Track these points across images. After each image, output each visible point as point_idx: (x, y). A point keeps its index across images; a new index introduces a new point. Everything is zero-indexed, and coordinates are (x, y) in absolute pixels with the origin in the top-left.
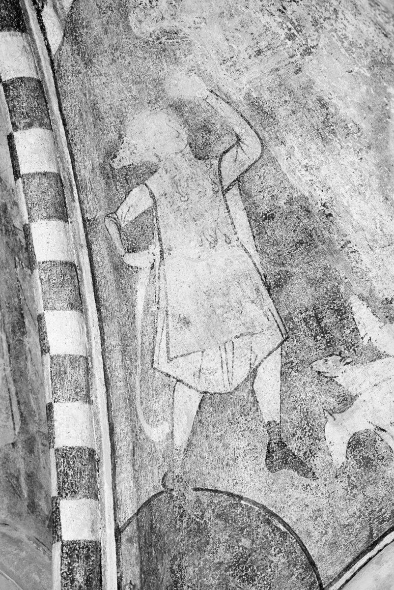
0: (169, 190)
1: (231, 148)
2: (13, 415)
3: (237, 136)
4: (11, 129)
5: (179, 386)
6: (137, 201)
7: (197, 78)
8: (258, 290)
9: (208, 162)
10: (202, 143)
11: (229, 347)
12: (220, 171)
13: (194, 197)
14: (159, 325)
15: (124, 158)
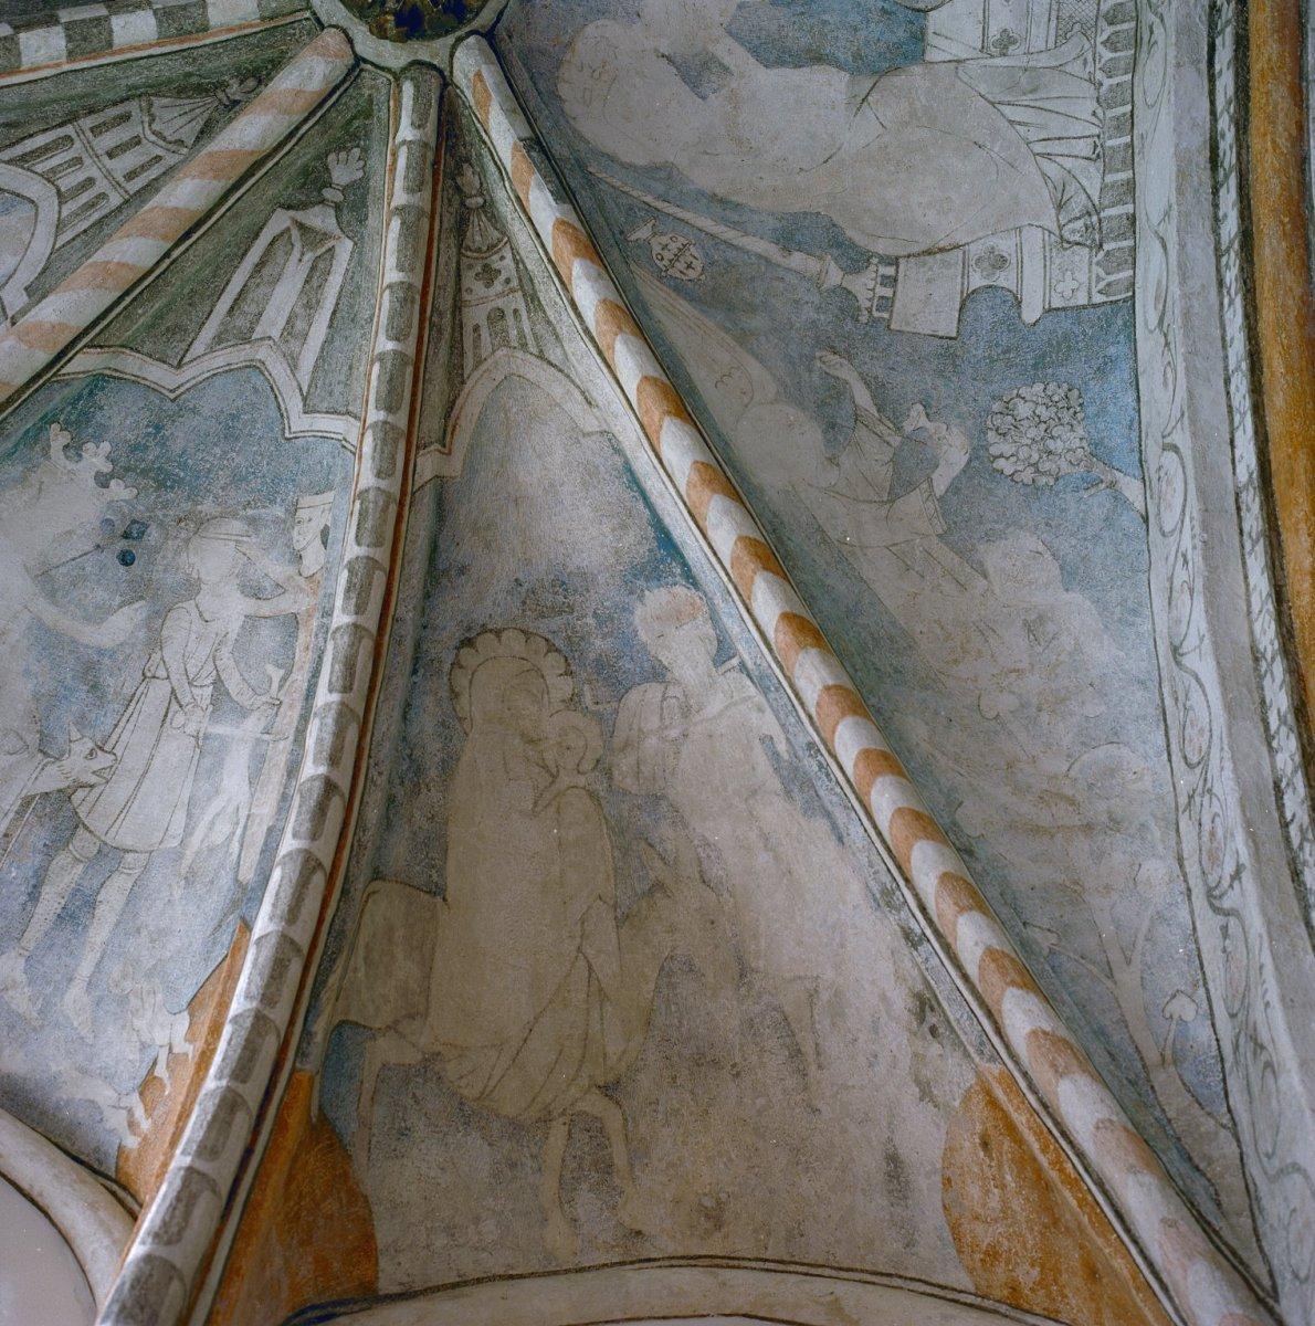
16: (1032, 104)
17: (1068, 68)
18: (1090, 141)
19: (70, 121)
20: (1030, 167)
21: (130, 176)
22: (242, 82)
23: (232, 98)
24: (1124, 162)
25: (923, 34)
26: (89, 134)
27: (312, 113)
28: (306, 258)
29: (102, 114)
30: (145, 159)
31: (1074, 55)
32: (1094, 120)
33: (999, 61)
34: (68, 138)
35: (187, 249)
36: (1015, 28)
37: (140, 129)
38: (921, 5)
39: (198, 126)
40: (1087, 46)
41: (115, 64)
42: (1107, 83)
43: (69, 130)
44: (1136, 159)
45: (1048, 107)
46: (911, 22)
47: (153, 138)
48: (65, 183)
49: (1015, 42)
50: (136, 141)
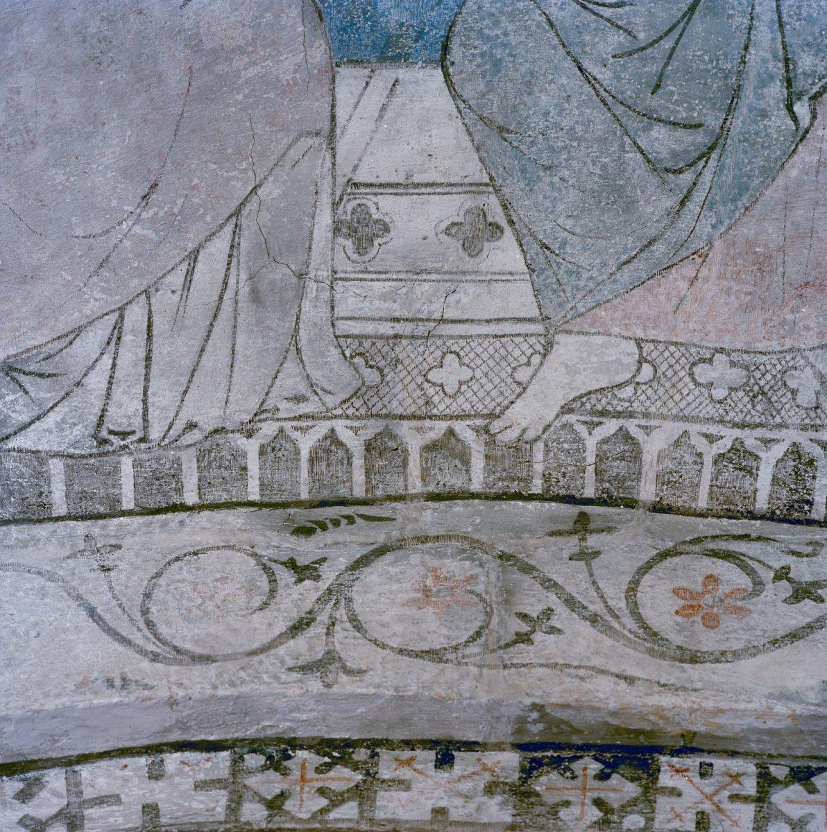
16: (229, 295)
17: (290, 366)
18: (137, 422)
20: (96, 300)
24: (84, 496)
25: (395, 59)
31: (316, 374)
32: (179, 425)
33: (325, 219)
36: (387, 250)
38: (456, 52)
40: (330, 401)
42: (251, 447)
44: (81, 528)
45: (217, 329)
46: (420, 35)
49: (360, 250)
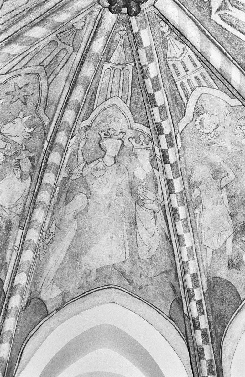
0: (205, 189)
1: (225, 176)
2: (125, 252)
3: (227, 173)
4: (172, 178)
5: (208, 248)
6: (196, 192)
7: (218, 156)
8: (228, 217)
9: (217, 180)
10: (216, 175)
11: (219, 235)
12: (220, 183)
13: (212, 191)
14: (202, 230)
15: (193, 179)
19: (175, 83)
21: (195, 65)
22: (162, 27)
23: (168, 30)
26: (179, 77)
27: (182, 8)
28: (231, 9)
29: (172, 73)
30: (189, 60)
34: (180, 83)
35: (229, 53)
37: (178, 61)
39: (178, 43)
41: (161, 72)
43: (178, 83)
47: (182, 57)
48: (195, 84)
50: (183, 63)
